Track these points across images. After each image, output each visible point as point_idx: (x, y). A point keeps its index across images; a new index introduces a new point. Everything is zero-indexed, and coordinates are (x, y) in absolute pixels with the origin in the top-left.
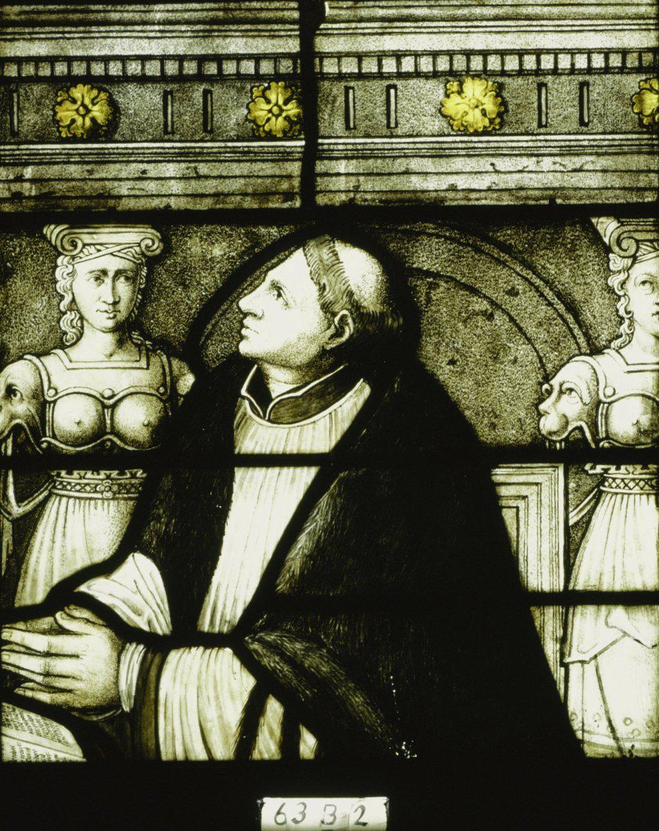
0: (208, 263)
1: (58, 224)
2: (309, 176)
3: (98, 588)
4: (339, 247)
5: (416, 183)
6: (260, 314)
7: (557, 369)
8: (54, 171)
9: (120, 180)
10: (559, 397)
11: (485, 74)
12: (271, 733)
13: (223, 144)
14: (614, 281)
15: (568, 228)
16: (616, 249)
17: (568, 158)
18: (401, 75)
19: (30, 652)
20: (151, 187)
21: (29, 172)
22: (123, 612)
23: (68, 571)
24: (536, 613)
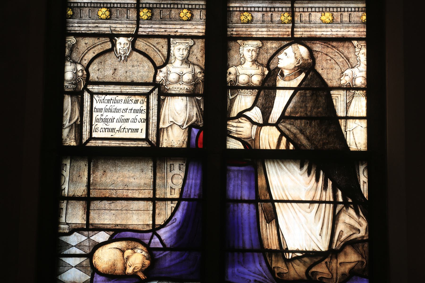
1: (240, 40)
2: (293, 32)
3: (247, 114)
4: (299, 45)
6: (282, 59)
8: (240, 29)
9: (253, 31)
10: (345, 77)
12: (284, 144)
13: (275, 25)
14: (356, 54)
15: (347, 43)
16: (357, 47)
17: (347, 29)
20: (260, 33)
21: (234, 29)
23: (241, 110)
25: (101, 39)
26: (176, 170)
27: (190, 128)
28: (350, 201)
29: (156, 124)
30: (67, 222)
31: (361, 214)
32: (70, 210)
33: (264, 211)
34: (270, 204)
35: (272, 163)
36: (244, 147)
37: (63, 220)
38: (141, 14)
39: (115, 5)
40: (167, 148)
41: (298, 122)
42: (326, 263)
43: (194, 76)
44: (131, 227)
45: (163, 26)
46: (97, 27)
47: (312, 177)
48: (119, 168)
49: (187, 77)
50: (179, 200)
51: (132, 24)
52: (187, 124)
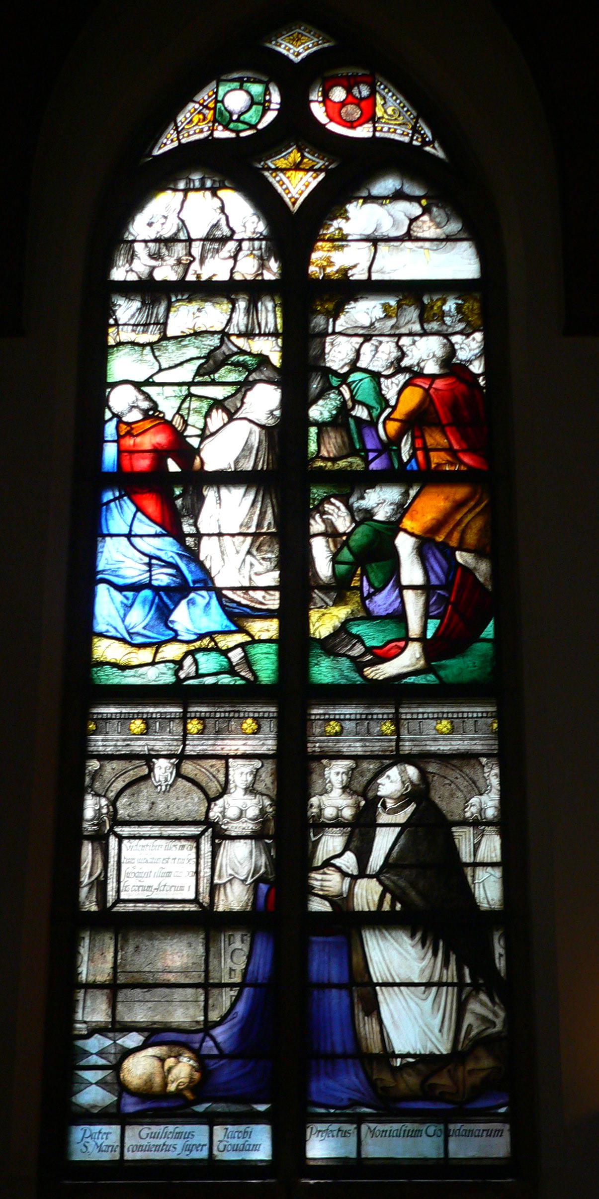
0: (369, 770)
2: (398, 746)
3: (336, 862)
4: (406, 765)
5: (428, 748)
7: (470, 799)
11: (447, 718)
14: (486, 775)
18: (423, 719)
19: (317, 880)
20: (353, 749)
21: (317, 745)
22: (344, 868)
23: (328, 857)
24: (465, 869)
25: (133, 761)
26: (238, 944)
27: (256, 883)
28: (481, 981)
29: (209, 878)
30: (85, 1019)
31: (497, 1000)
32: (88, 1003)
33: (361, 998)
34: (369, 988)
35: (372, 931)
36: (333, 909)
37: (79, 1016)
38: (189, 726)
39: (154, 716)
40: (224, 912)
41: (407, 872)
42: (449, 1071)
43: (262, 811)
44: (174, 1025)
45: (219, 742)
46: (128, 745)
47: (428, 951)
48: (157, 942)
49: (253, 812)
50: (241, 986)
51: (176, 740)
52: (252, 877)
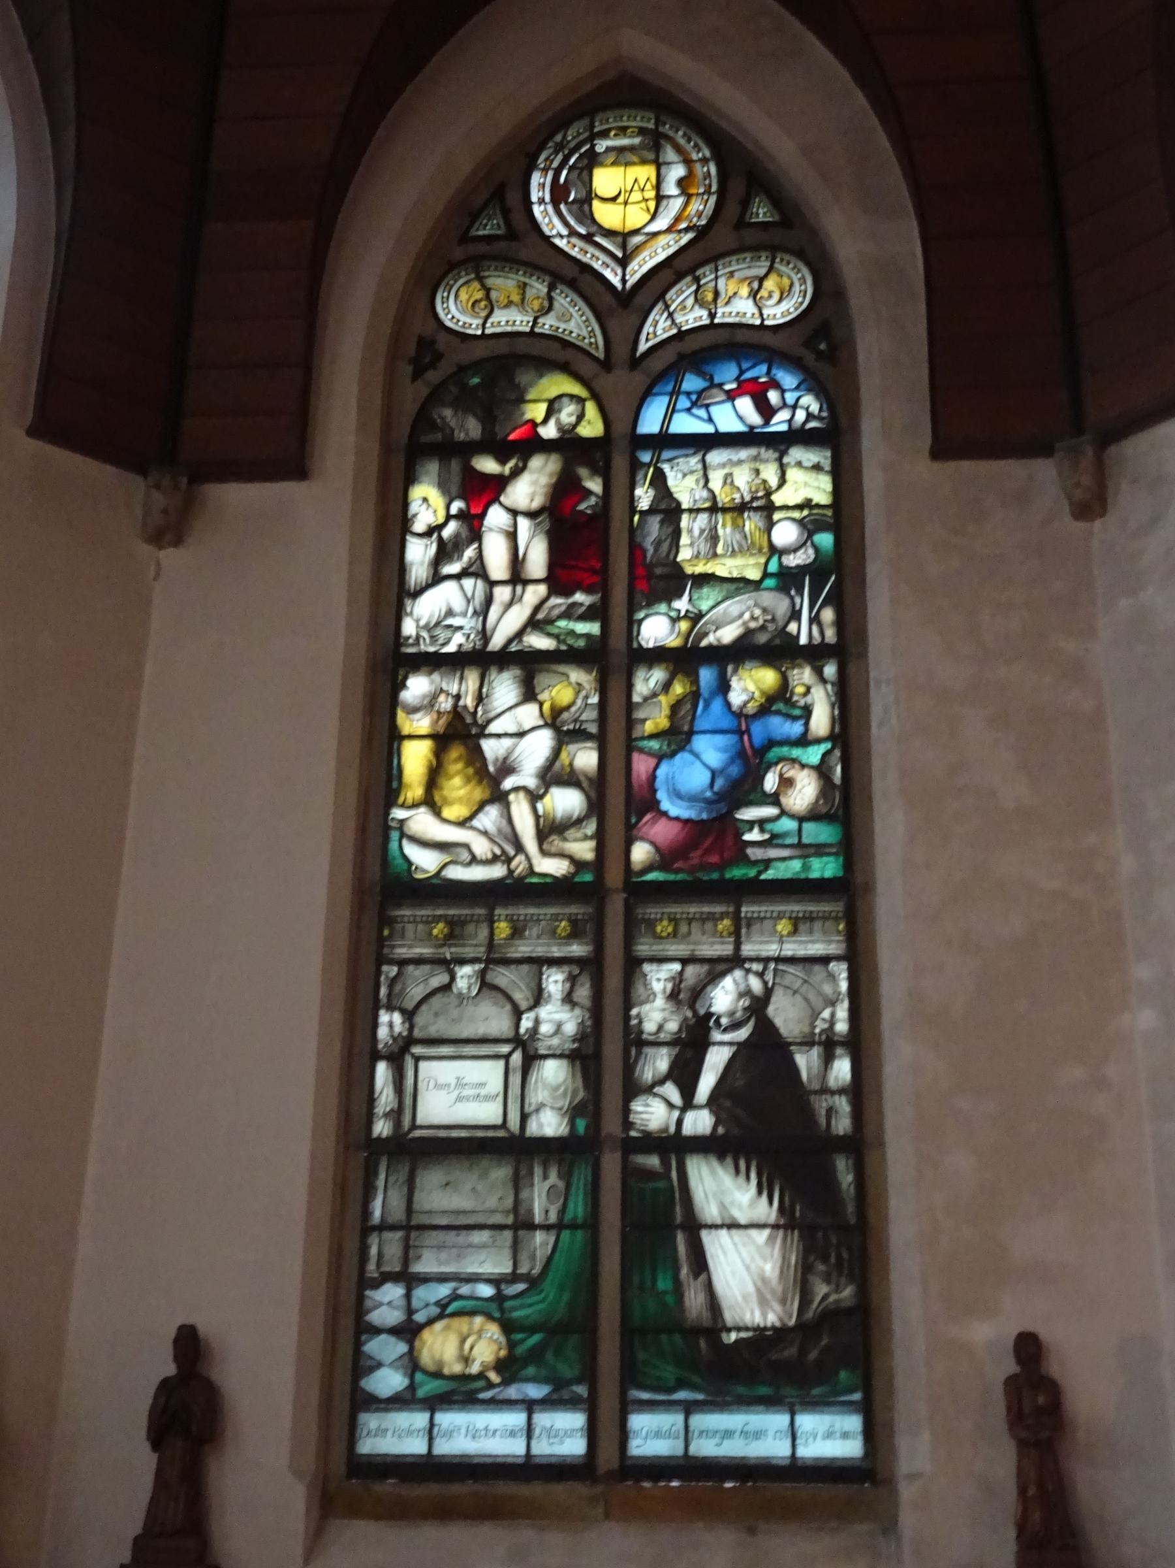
49: (570, 1028)
